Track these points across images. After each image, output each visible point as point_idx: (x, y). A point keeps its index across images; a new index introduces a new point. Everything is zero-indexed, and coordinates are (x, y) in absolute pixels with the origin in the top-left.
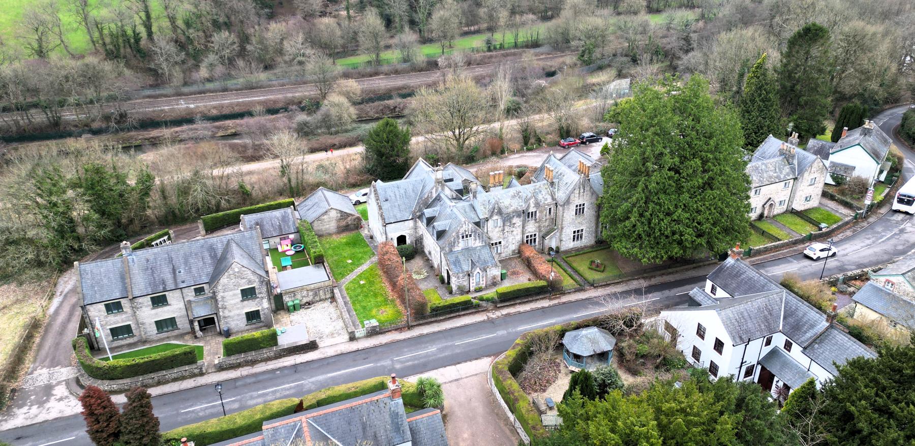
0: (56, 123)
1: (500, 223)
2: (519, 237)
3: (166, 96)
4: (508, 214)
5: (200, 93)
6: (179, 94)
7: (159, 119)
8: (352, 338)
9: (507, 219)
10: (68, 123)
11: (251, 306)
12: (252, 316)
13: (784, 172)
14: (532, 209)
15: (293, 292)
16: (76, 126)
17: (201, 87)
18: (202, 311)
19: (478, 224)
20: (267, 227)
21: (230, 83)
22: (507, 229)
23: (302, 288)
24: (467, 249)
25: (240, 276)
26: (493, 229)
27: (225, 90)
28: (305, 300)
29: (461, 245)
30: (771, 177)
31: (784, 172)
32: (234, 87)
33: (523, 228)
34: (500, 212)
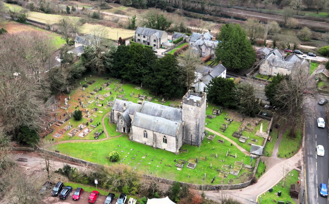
0: (203, 9)
1: (205, 48)
2: (209, 53)
3: (241, 9)
4: (207, 46)
5: (252, 11)
6: (245, 10)
7: (228, 15)
8: (162, 54)
9: (207, 47)
10: (206, 10)
11: (155, 43)
12: (155, 45)
13: (289, 67)
14: (213, 47)
15: (164, 45)
16: (208, 11)
17: (256, 10)
18: (148, 41)
19: (199, 46)
20: (177, 36)
21: (264, 10)
22: (207, 50)
23: (166, 45)
24: (194, 50)
25: (154, 36)
26: (203, 48)
27: (260, 12)
28: (166, 48)
29: (193, 48)
30: (283, 66)
31: (289, 67)
32: (264, 12)
33: (211, 51)
34: (205, 45)
